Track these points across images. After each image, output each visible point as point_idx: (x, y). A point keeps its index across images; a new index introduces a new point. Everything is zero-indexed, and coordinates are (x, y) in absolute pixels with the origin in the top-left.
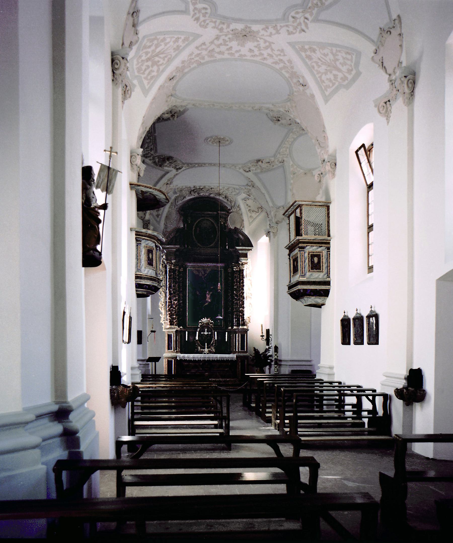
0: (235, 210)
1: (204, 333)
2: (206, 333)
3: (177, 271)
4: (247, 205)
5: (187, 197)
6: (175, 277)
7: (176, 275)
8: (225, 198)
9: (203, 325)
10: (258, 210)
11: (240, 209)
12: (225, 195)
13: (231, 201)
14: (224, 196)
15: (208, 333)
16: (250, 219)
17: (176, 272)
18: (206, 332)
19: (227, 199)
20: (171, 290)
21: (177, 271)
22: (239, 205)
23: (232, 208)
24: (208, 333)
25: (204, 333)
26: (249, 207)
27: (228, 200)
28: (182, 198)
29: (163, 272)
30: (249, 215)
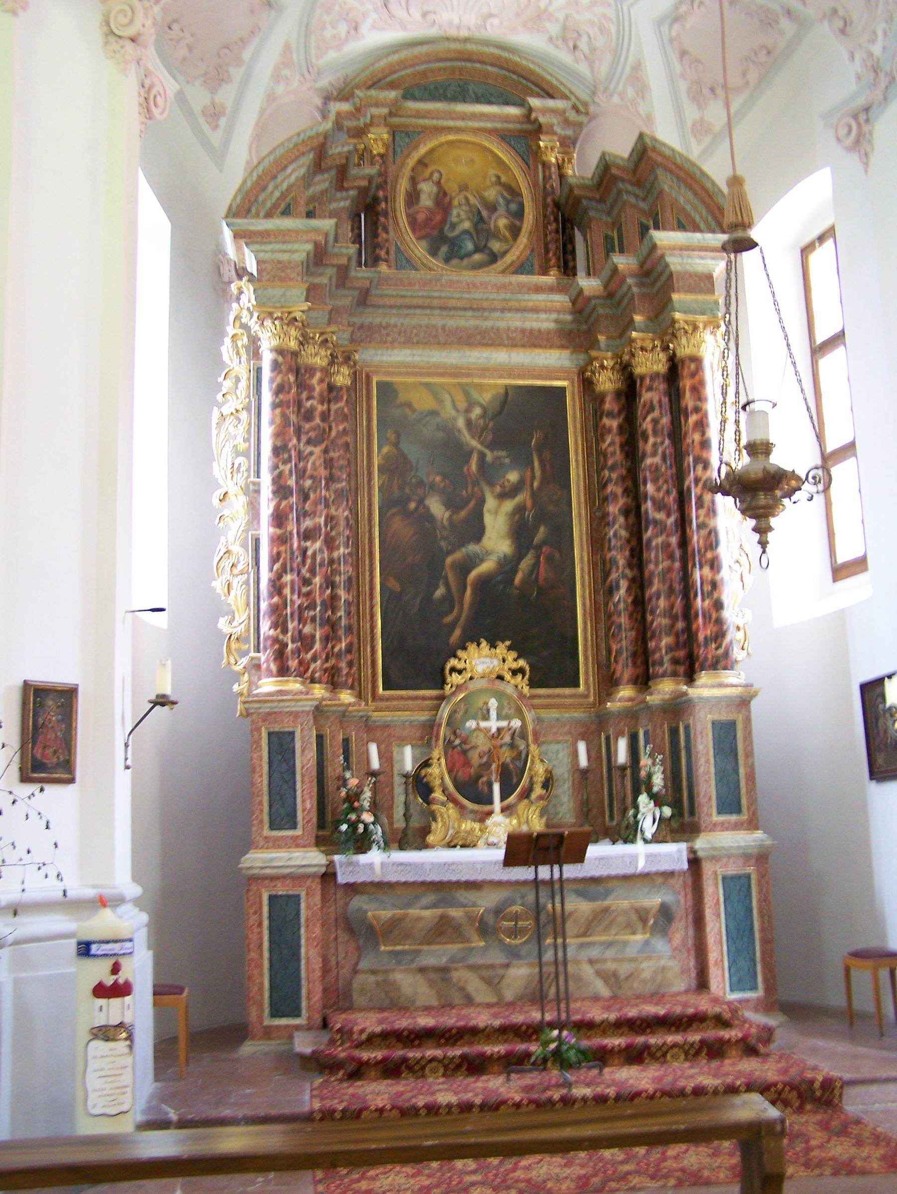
0: (616, 99)
1: (483, 724)
2: (493, 724)
3: (318, 375)
4: (683, 53)
5: (365, 28)
6: (308, 404)
7: (308, 399)
8: (560, 43)
9: (472, 686)
10: (744, 74)
11: (643, 90)
12: (561, 16)
13: (593, 50)
14: (554, 29)
15: (504, 724)
16: (692, 140)
17: (315, 381)
18: (493, 714)
19: (571, 45)
20: (286, 468)
21: (318, 375)
22: (638, 67)
23: (594, 93)
24: (504, 724)
25: (483, 724)
26: (698, 61)
27: (575, 47)
28: (343, 28)
29: (238, 380)
30: (691, 113)
